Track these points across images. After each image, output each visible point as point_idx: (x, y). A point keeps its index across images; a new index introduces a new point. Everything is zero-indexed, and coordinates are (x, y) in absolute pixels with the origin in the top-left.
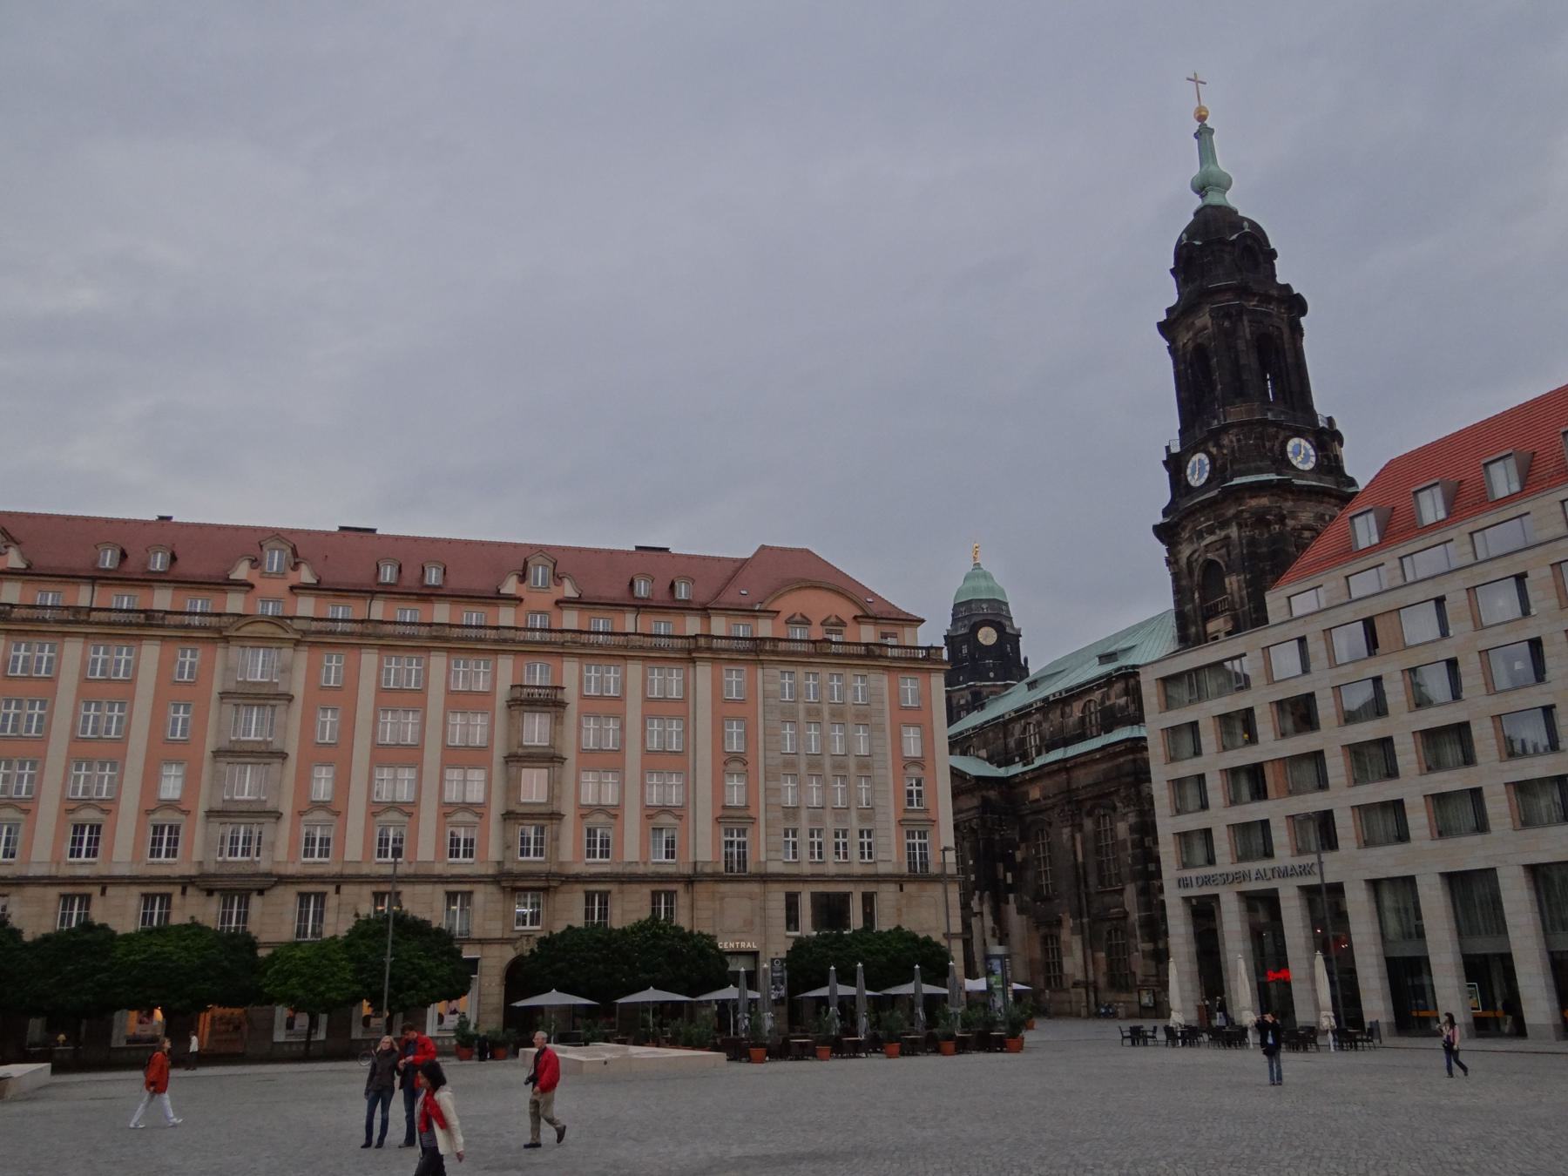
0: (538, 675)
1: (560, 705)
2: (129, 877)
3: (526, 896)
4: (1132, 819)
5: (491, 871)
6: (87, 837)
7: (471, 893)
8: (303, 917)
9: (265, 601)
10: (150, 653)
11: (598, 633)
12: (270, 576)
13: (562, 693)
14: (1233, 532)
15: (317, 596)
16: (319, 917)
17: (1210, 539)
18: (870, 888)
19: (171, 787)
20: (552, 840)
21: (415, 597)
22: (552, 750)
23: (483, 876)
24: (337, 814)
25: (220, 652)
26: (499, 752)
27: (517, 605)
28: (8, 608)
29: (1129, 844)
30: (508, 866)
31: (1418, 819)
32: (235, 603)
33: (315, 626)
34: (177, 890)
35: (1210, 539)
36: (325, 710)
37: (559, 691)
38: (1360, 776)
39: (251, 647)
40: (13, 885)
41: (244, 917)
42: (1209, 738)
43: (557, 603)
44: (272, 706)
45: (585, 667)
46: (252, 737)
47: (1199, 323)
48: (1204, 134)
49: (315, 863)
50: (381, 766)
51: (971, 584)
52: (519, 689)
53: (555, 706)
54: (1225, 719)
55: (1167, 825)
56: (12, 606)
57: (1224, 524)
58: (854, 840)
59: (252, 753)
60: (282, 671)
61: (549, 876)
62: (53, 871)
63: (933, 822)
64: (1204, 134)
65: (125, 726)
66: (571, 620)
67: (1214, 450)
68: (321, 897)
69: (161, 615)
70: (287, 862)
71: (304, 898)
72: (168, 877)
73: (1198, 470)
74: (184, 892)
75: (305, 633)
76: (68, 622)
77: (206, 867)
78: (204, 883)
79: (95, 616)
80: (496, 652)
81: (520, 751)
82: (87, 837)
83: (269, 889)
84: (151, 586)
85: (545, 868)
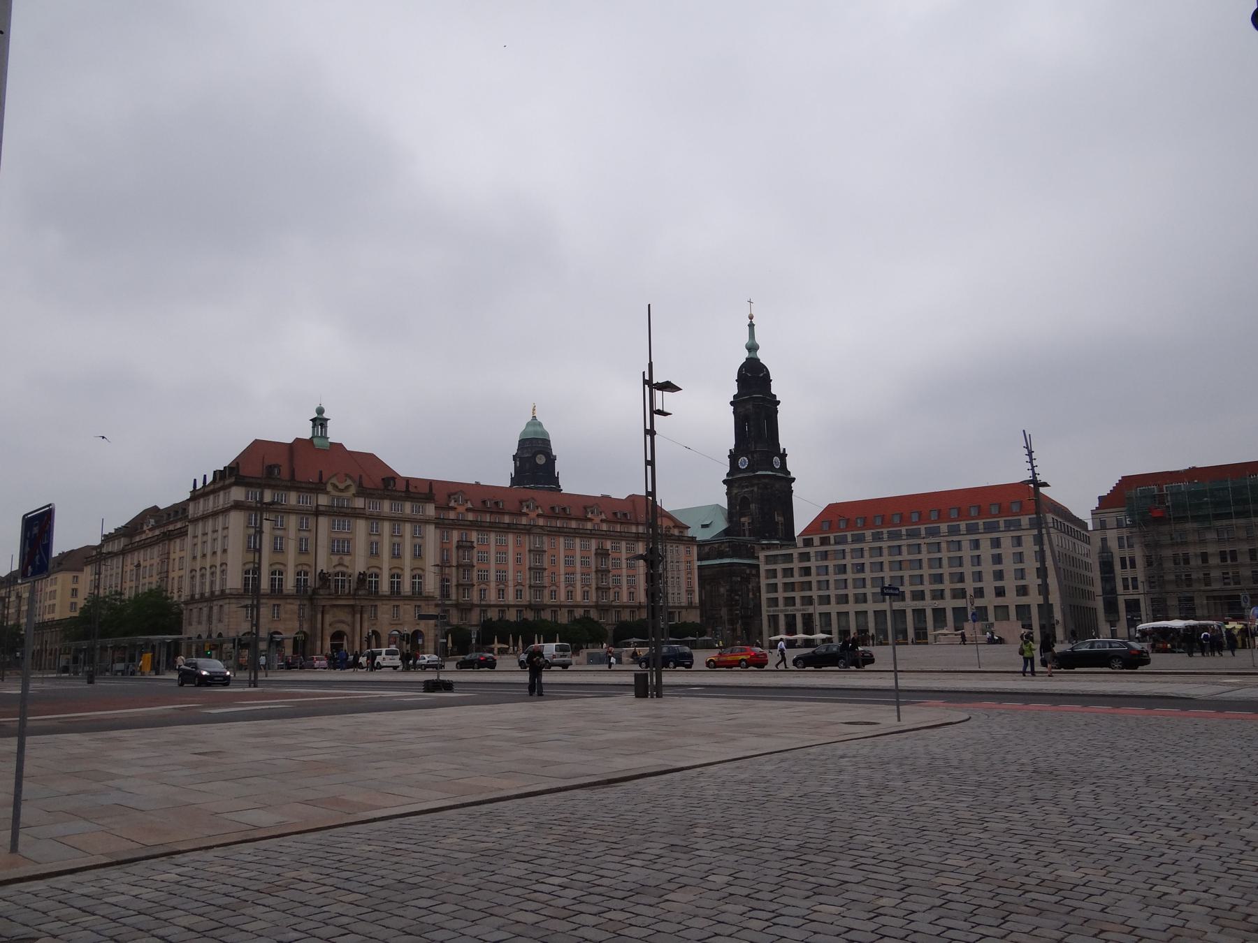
4: (728, 587)
5: (594, 604)
6: (501, 592)
14: (756, 489)
17: (746, 490)
18: (680, 610)
24: (558, 587)
29: (725, 596)
31: (833, 600)
34: (524, 609)
35: (746, 490)
38: (785, 576)
42: (780, 574)
47: (748, 407)
48: (751, 326)
51: (531, 429)
54: (785, 570)
55: (765, 596)
57: (753, 485)
58: (676, 595)
63: (694, 591)
64: (751, 326)
67: (750, 458)
68: (555, 611)
73: (743, 462)
78: (530, 607)
82: (501, 592)
85: (607, 604)
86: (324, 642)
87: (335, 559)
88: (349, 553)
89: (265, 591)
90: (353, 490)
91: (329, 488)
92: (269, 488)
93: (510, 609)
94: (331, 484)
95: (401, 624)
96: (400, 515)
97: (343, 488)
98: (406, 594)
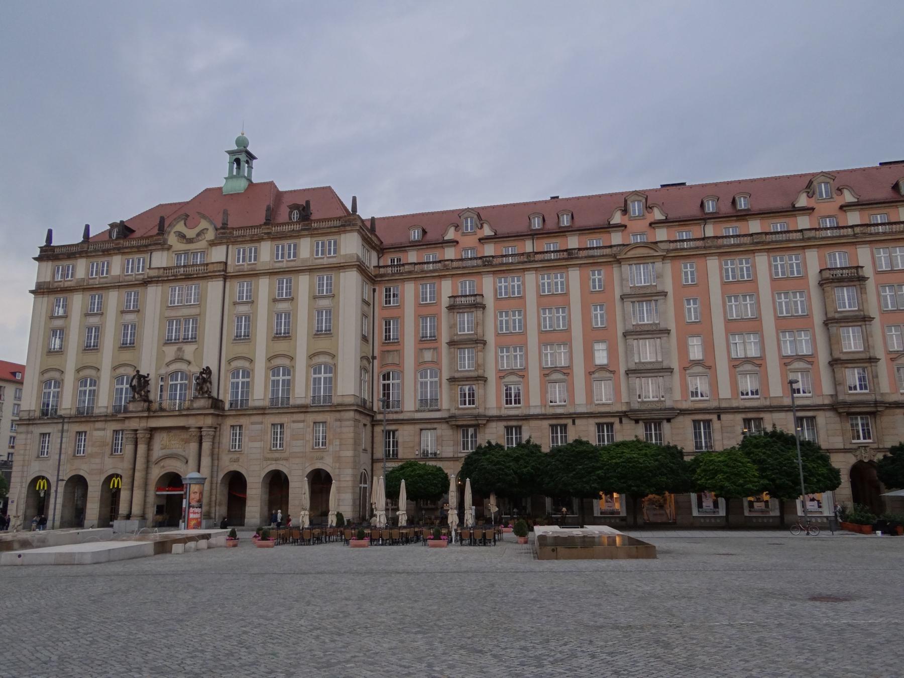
0: (839, 259)
1: (862, 279)
2: (587, 413)
3: (857, 419)
5: (827, 402)
7: (814, 417)
8: (697, 435)
9: (635, 235)
10: (574, 275)
11: (877, 225)
12: (635, 219)
13: (862, 271)
15: (668, 227)
16: (709, 435)
19: (601, 357)
20: (873, 377)
21: (735, 218)
22: (862, 313)
23: (819, 406)
24: (709, 368)
25: (615, 270)
26: (818, 318)
27: (810, 214)
28: (491, 258)
30: (841, 398)
32: (616, 238)
33: (672, 246)
34: (616, 420)
36: (688, 301)
37: (859, 269)
39: (635, 264)
40: (523, 420)
41: (659, 437)
43: (841, 207)
44: (656, 301)
45: (875, 250)
46: (646, 322)
49: (700, 401)
50: (734, 334)
52: (828, 271)
53: (859, 280)
56: (493, 257)
59: (648, 332)
60: (658, 277)
61: (876, 403)
62: (543, 412)
65: (568, 321)
66: (854, 218)
68: (708, 423)
69: (576, 251)
70: (681, 400)
71: (696, 423)
72: (609, 413)
74: (621, 422)
75: (668, 251)
76: (526, 262)
77: (632, 405)
79: (538, 257)
80: (804, 248)
81: (837, 316)
83: (673, 418)
84: (565, 235)
85: (871, 398)
86: (129, 498)
87: (171, 352)
88: (194, 340)
89: (68, 412)
90: (210, 235)
91: (172, 239)
92: (81, 257)
93: (577, 421)
94: (175, 232)
95: (286, 459)
96: (293, 264)
97: (194, 236)
98: (299, 402)
